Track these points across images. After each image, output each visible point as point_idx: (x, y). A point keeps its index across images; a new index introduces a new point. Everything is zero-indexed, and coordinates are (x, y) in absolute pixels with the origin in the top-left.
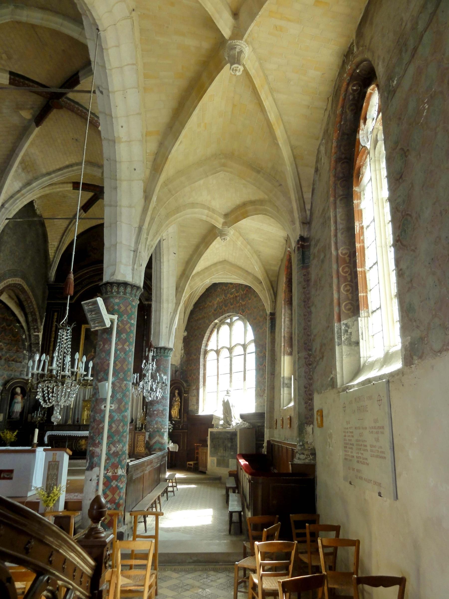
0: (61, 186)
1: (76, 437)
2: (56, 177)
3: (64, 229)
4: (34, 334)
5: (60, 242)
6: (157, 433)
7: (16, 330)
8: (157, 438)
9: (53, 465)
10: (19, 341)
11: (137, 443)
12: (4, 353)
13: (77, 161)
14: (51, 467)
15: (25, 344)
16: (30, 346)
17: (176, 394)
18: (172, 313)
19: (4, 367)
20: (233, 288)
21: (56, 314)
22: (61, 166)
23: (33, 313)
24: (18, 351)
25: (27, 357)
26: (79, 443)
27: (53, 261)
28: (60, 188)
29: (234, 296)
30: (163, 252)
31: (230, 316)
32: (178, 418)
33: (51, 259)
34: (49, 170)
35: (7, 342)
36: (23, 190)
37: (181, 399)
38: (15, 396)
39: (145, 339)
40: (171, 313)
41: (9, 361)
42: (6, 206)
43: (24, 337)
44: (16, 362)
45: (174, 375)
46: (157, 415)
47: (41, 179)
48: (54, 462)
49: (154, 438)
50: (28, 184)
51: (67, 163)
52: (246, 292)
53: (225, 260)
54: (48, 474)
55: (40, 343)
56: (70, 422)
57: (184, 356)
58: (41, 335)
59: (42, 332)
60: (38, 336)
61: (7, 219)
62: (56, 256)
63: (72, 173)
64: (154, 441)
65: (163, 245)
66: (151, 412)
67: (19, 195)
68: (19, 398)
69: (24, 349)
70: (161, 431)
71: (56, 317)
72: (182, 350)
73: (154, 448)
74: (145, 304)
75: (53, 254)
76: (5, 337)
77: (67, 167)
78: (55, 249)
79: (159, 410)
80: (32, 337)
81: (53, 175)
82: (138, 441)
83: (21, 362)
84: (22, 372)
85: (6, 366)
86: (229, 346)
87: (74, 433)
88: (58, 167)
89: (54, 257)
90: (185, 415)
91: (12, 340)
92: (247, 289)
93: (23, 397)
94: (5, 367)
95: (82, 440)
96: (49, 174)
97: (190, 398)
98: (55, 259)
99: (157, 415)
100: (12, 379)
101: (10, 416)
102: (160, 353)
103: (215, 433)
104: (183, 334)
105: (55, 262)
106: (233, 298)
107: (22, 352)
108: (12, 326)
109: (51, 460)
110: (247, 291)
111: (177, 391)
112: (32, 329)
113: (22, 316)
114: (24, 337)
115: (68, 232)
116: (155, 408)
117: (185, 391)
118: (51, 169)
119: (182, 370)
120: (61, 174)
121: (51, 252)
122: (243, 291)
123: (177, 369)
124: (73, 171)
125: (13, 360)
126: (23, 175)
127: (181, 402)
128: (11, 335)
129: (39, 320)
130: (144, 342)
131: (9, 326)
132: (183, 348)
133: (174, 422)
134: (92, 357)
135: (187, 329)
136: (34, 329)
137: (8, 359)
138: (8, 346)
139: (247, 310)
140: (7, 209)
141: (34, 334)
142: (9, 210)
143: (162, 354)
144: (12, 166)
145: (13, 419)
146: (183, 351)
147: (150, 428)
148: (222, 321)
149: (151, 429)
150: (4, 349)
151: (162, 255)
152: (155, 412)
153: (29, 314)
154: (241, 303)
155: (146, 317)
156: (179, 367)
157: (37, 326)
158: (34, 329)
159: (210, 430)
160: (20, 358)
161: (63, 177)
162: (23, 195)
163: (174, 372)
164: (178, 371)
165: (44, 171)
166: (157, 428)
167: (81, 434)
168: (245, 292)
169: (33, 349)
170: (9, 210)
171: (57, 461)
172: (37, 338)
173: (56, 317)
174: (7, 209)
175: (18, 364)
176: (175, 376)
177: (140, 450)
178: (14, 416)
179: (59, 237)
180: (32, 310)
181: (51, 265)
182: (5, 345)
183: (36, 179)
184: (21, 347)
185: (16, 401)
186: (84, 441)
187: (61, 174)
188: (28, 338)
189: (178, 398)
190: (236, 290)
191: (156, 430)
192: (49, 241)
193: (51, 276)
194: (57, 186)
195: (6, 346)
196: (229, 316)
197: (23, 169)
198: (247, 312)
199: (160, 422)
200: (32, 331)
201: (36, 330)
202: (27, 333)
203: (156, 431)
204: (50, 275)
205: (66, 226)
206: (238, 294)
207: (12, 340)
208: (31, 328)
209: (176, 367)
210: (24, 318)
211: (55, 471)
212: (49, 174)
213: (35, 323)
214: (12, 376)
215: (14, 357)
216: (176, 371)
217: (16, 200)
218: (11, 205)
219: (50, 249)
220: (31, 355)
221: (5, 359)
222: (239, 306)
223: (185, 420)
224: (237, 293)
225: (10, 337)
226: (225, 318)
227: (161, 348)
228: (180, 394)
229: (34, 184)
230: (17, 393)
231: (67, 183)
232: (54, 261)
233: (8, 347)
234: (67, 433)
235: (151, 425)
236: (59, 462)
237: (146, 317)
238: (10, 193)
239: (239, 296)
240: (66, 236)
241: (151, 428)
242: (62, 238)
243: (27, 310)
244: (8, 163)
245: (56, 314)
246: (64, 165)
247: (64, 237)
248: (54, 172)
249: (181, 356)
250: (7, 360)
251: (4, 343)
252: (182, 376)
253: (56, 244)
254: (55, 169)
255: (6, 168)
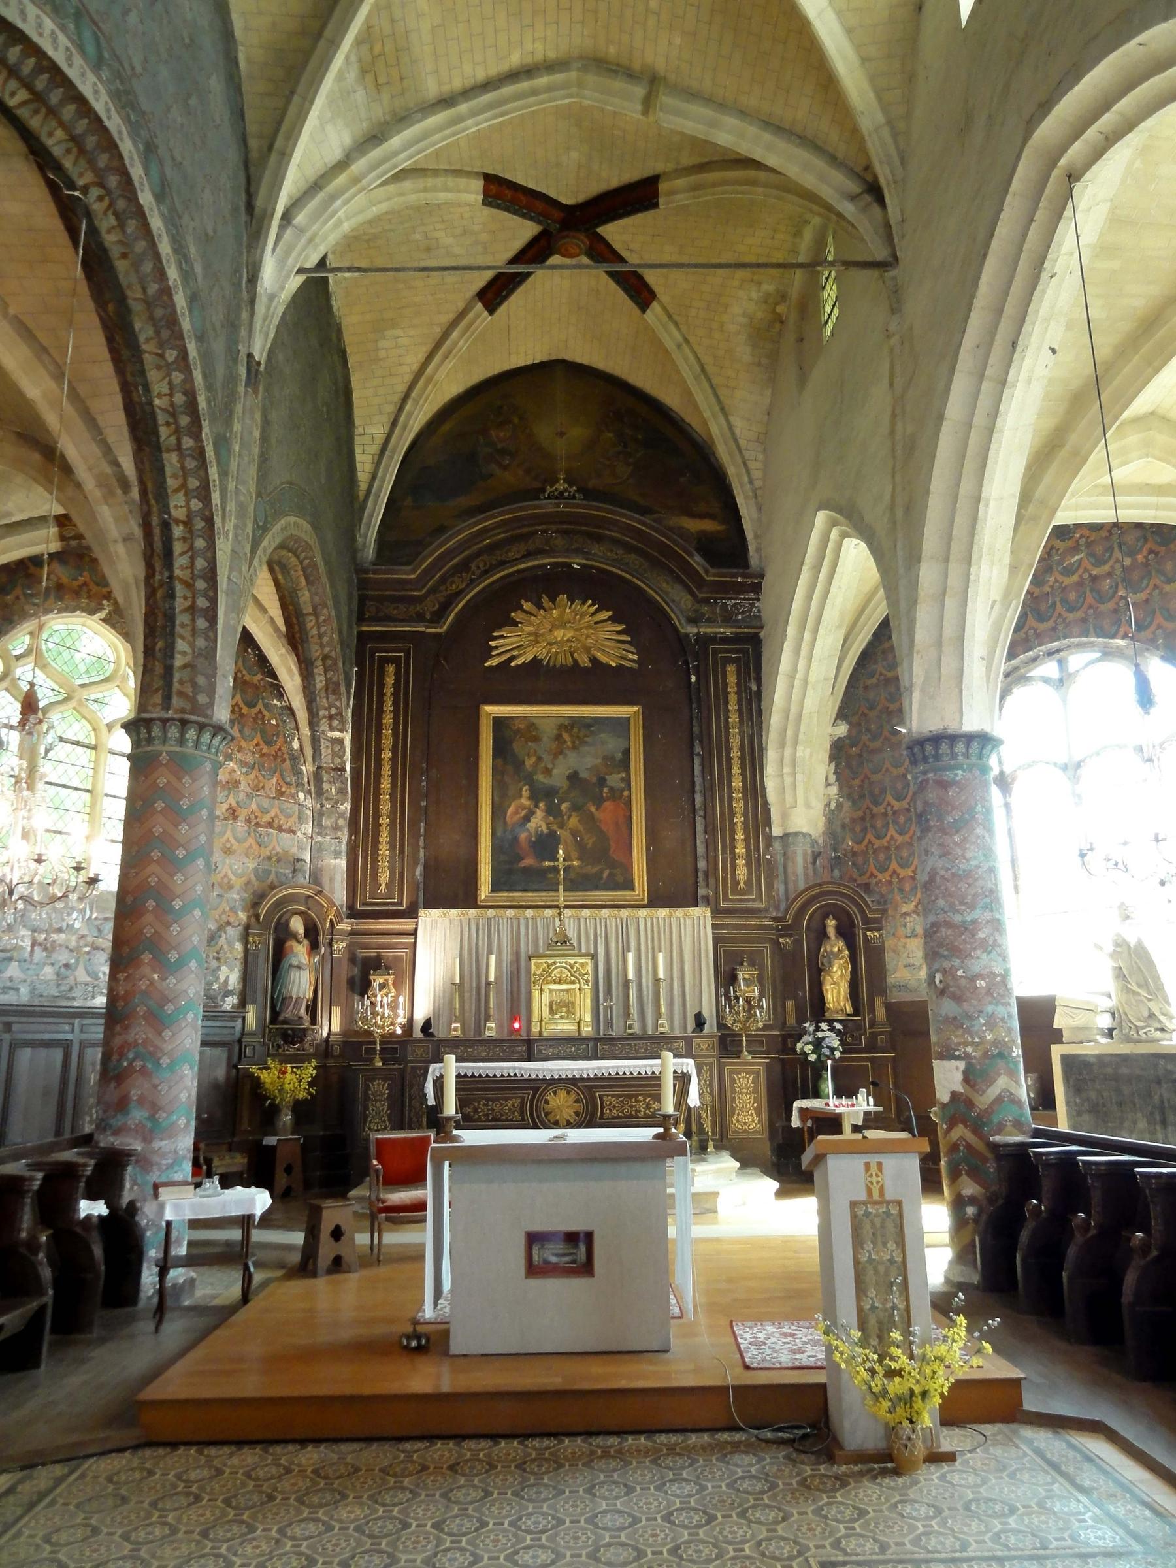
0: (451, 181)
1: (537, 1080)
2: (474, 113)
3: (408, 378)
4: (330, 734)
5: (394, 424)
6: (1001, 1063)
7: (273, 722)
8: (1002, 1082)
9: (878, 1222)
10: (284, 761)
11: (733, 1100)
12: (242, 796)
13: (552, 55)
14: (867, 1229)
15: (300, 772)
16: (317, 777)
17: (831, 931)
18: (997, 606)
19: (246, 845)
20: (1075, 549)
21: (391, 669)
22: (495, 68)
23: (329, 662)
24: (282, 794)
25: (309, 813)
26: (547, 1102)
27: (369, 491)
28: (447, 190)
29: (1086, 576)
30: (1031, 334)
31: (1058, 651)
32: (849, 1009)
33: (363, 486)
34: (446, 88)
35: (250, 759)
36: (358, 159)
37: (851, 946)
38: (288, 944)
39: (698, 749)
40: (994, 602)
41: (257, 824)
42: (300, 219)
43: (296, 745)
44: (280, 829)
45: (810, 866)
46: (989, 992)
47: (419, 121)
48: (875, 1203)
49: (991, 1082)
50: (374, 138)
51: (515, 59)
52: (1146, 557)
53: (1152, 413)
54: (857, 1262)
55: (348, 768)
56: (491, 1029)
57: (839, 806)
58: (347, 737)
59: (350, 731)
60: (340, 742)
61: (301, 271)
62: (380, 474)
63: (531, 100)
64: (993, 1092)
65: (1041, 299)
66: (963, 982)
67: (341, 179)
68: (300, 951)
69: (299, 785)
70: (1010, 1054)
71: (390, 680)
72: (828, 784)
73: (995, 1120)
74: (682, 639)
75: (369, 468)
76: (243, 744)
77: (513, 76)
78: (375, 449)
79: (992, 974)
80: (324, 744)
81: (463, 108)
82: (733, 1091)
83: (294, 833)
84: (298, 865)
85: (251, 841)
86: (1063, 759)
87: (526, 1069)
88: (481, 75)
89: (374, 477)
90: (878, 1000)
91: (263, 755)
92: (1148, 546)
93: (314, 946)
94: (250, 847)
95: (555, 1093)
96: (446, 102)
97: (889, 943)
98: (377, 483)
99: (989, 992)
100: (272, 887)
101: (275, 1015)
102: (967, 755)
103: (1092, 1060)
104: (830, 730)
105: (377, 496)
106: (1080, 584)
107: (294, 796)
108: (260, 706)
109: (863, 1197)
110: (1151, 551)
111: (831, 923)
112: (325, 717)
113: (290, 670)
114: (296, 745)
115: (426, 386)
116: (976, 967)
117: (866, 921)
118: (457, 84)
119: (835, 851)
120: (490, 106)
121: (364, 459)
122: (1132, 553)
123: (816, 849)
124: (534, 92)
125: (270, 824)
126: (360, 96)
127: (853, 959)
128: (258, 738)
129: (343, 689)
130: (697, 761)
131: (251, 705)
132: (832, 778)
133: (838, 1026)
134: (524, 813)
135: (842, 714)
136: (331, 717)
137: (256, 817)
138: (255, 773)
139: (1159, 619)
140: (301, 230)
141: (330, 734)
142: (309, 234)
143: (973, 759)
144: (335, 44)
145: (285, 1022)
146: (834, 790)
147: (966, 1044)
148: (1017, 674)
149: (969, 1049)
150: (243, 786)
151: (1019, 349)
152: (981, 983)
153: (319, 663)
154: (1122, 597)
155: (693, 679)
156: (820, 841)
157: (337, 708)
158: (331, 717)
159: (1057, 1051)
160: (290, 816)
161: (496, 117)
162: (356, 180)
163: (810, 859)
164: (819, 854)
165: (432, 88)
166: (995, 1043)
167: (551, 1070)
168: (1140, 558)
169: (326, 786)
170: (309, 234)
171: (888, 1203)
172: (337, 748)
173: (390, 680)
174: (301, 230)
175: (285, 835)
176: (815, 870)
177: (745, 1123)
178: (287, 1014)
179: (391, 409)
180: (327, 650)
181: (363, 508)
182: (244, 770)
183: (401, 119)
184: (288, 779)
185: (295, 962)
186: (562, 1094)
187: (490, 106)
188: (309, 752)
189: (836, 945)
190: (1092, 554)
191: (995, 1051)
192: (357, 421)
193: (364, 544)
194: (439, 181)
195: (246, 774)
196: (1050, 654)
197: (363, 72)
198: (1159, 627)
199: (1002, 1019)
200: (324, 726)
201: (335, 723)
202: (306, 731)
203: (993, 1056)
204: (360, 540)
205: (415, 367)
206: (1107, 568)
207: (263, 755)
208: (322, 713)
209: (814, 842)
210: (298, 680)
211: (891, 1245)
212: (446, 102)
213: (332, 698)
214: (272, 877)
215: (273, 814)
216: (816, 856)
217: (333, 198)
218: (316, 216)
219: (358, 450)
220: (322, 806)
221: (248, 821)
222: (1115, 611)
223: (881, 1016)
224: (1099, 562)
225: (257, 745)
226: (1034, 660)
227: (970, 738)
228: (847, 933)
229: (396, 141)
230: (294, 936)
231: (468, 174)
232: (374, 490)
233: (252, 776)
234: (502, 1068)
235: (968, 1031)
236: (899, 1203)
237: (693, 679)
238: (311, 174)
239: (1110, 574)
240: (416, 402)
241: (973, 1044)
242: (401, 409)
243: (315, 651)
244: (319, 35)
245: (391, 669)
246: (504, 67)
247: (408, 407)
248: (468, 93)
249: (828, 805)
250: (253, 823)
251: (243, 764)
252: (837, 873)
253: (378, 431)
254: (469, 83)
255: (307, 54)
